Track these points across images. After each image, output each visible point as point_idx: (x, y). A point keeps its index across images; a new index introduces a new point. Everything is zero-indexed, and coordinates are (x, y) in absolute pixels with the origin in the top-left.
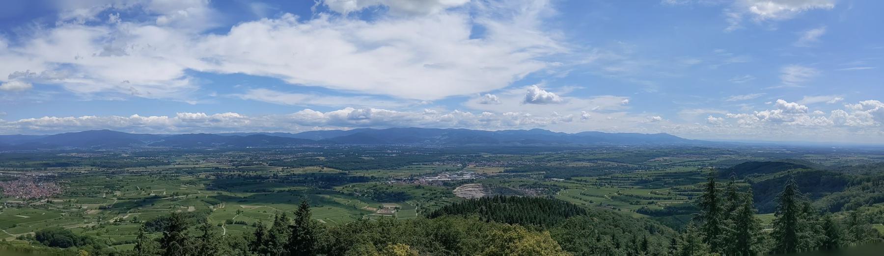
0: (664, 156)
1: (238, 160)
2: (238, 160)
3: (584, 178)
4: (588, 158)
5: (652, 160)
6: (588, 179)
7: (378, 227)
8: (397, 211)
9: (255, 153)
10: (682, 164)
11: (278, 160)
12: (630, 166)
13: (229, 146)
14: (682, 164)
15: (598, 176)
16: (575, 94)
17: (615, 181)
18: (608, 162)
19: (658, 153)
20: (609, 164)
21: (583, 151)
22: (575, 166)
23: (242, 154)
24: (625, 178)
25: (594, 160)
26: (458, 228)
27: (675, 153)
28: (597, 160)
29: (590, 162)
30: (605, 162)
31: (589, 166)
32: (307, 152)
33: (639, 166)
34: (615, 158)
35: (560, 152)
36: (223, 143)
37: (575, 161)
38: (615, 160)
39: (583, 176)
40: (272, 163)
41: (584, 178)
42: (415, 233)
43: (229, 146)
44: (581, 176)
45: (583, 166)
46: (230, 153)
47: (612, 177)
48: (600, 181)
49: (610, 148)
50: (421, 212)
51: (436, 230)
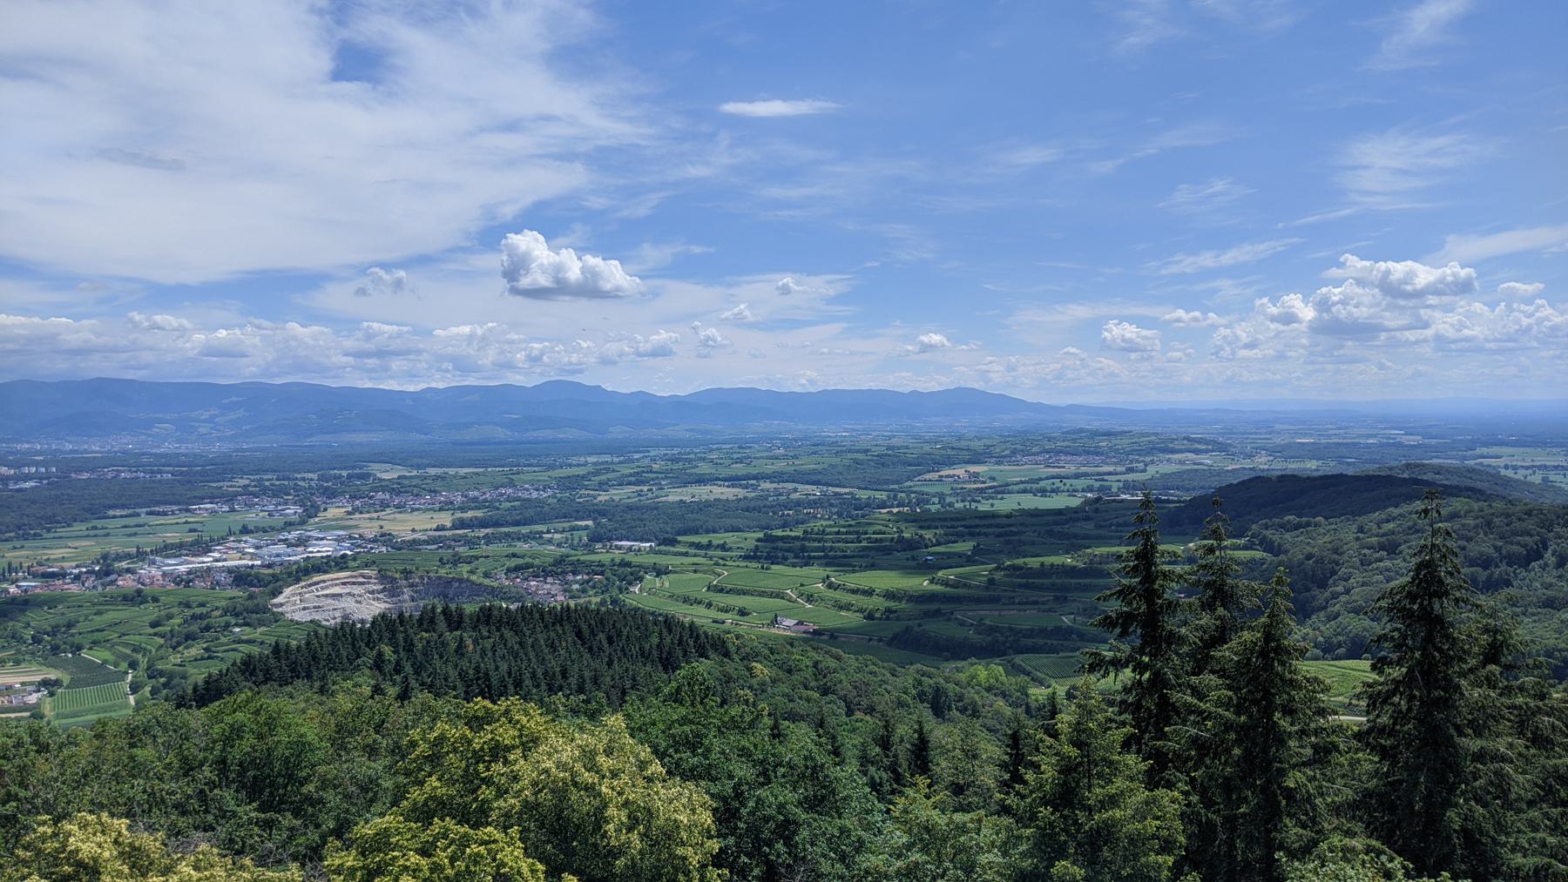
0: (969, 462)
3: (717, 539)
4: (724, 472)
5: (928, 476)
6: (731, 538)
10: (1029, 486)
12: (863, 495)
14: (1029, 486)
15: (762, 528)
16: (682, 269)
17: (816, 544)
18: (790, 486)
19: (950, 452)
20: (796, 490)
21: (711, 451)
22: (688, 499)
24: (847, 533)
25: (747, 477)
27: (1007, 452)
28: (755, 477)
29: (733, 486)
30: (782, 485)
31: (731, 498)
33: (892, 494)
34: (815, 472)
35: (637, 456)
37: (685, 484)
38: (814, 478)
39: (714, 531)
41: (717, 539)
44: (708, 532)
45: (712, 498)
47: (805, 532)
48: (772, 545)
49: (796, 440)
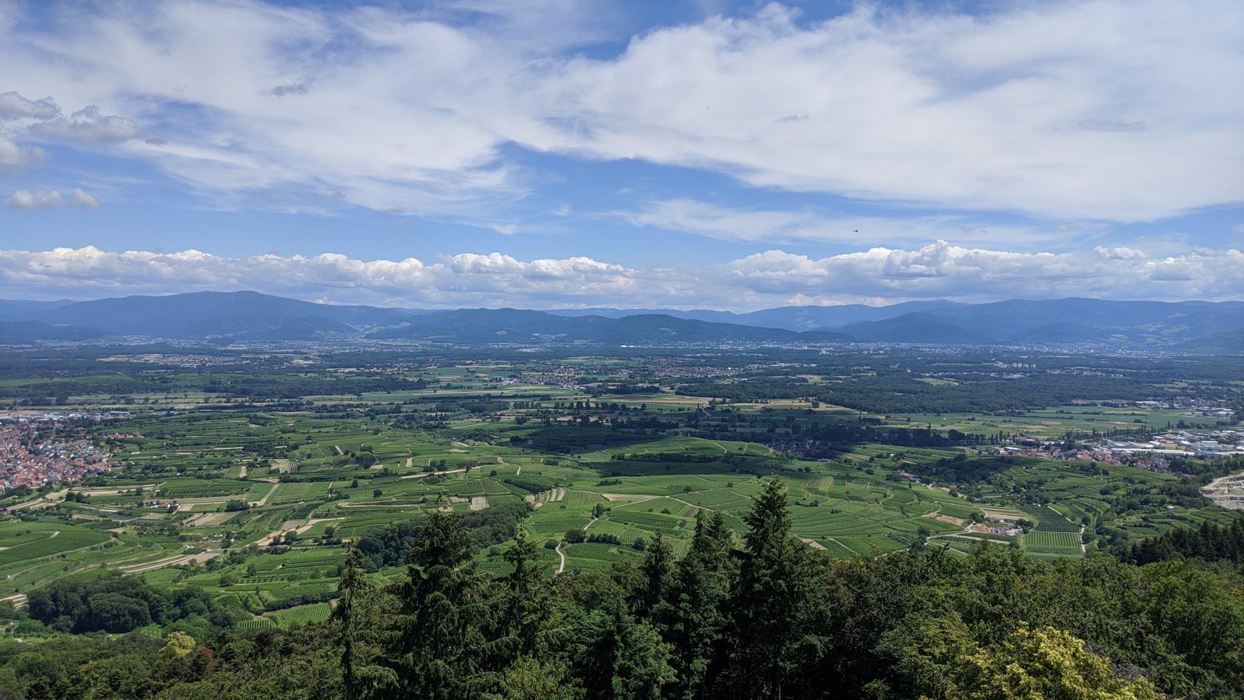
1: (600, 378)
2: (600, 378)
7: (976, 572)
8: (1025, 532)
9: (643, 360)
11: (701, 381)
13: (576, 342)
23: (609, 362)
26: (1230, 604)
32: (774, 360)
36: (563, 335)
40: (685, 388)
42: (1088, 603)
43: (576, 342)
46: (580, 360)
50: (1096, 541)
51: (1154, 600)
